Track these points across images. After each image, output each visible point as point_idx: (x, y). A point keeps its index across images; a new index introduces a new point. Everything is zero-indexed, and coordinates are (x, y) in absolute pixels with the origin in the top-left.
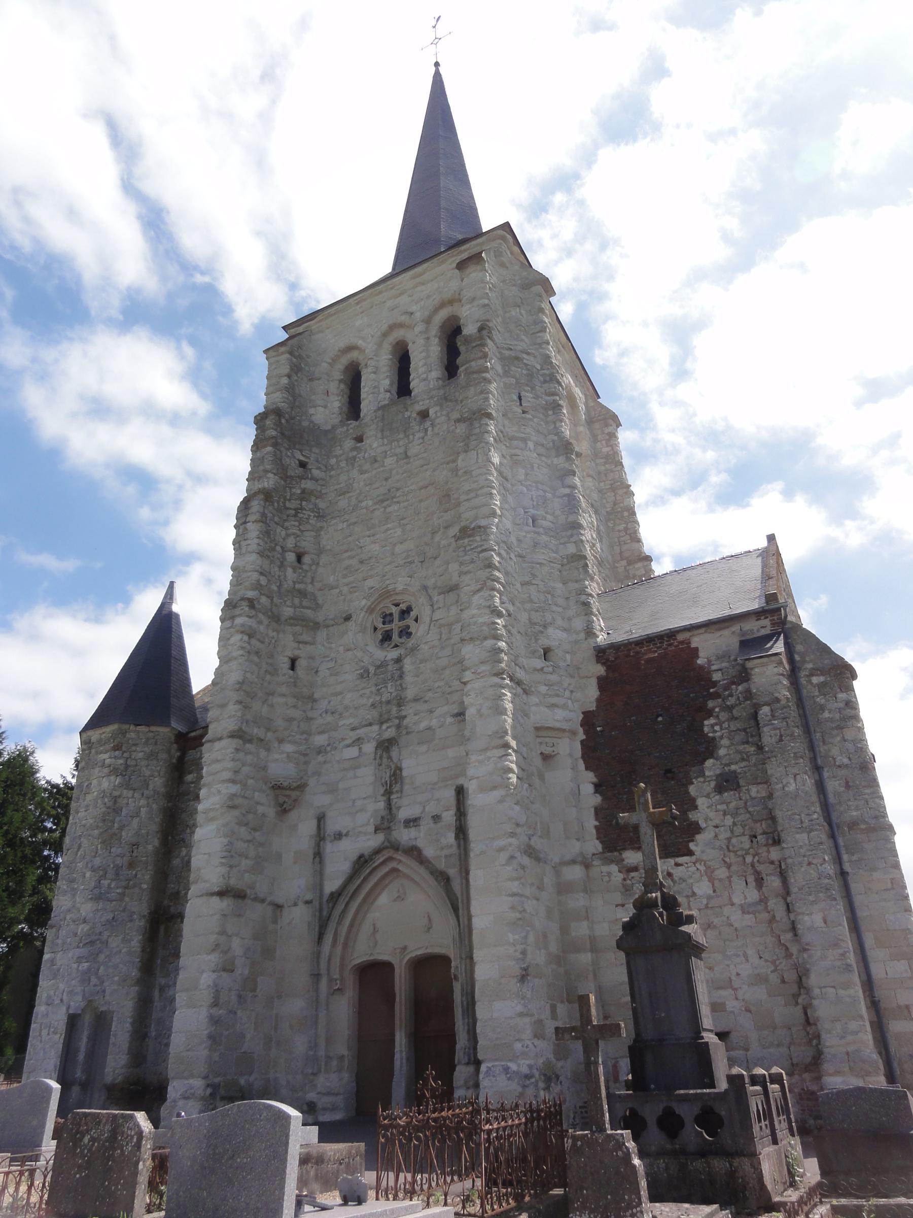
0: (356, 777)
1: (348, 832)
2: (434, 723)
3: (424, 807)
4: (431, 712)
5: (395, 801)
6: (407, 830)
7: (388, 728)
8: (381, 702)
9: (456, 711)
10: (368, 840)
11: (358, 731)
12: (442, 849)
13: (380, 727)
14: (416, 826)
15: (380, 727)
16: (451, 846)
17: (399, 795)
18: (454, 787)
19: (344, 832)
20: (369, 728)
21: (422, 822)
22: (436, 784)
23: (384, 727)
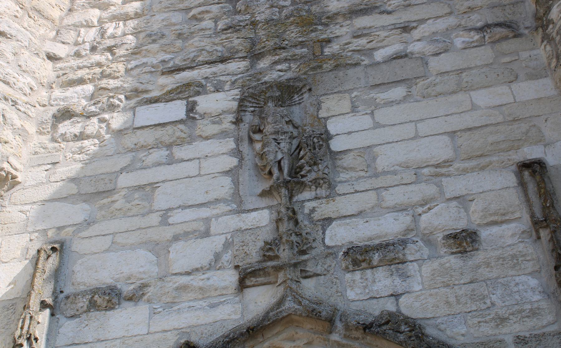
0: (171, 161)
1: (144, 286)
2: (416, 47)
3: (416, 218)
4: (406, 29)
5: (309, 205)
6: (358, 275)
7: (276, 63)
8: (254, 24)
9: (479, 24)
10: (213, 306)
11: (187, 75)
12: (502, 320)
13: (252, 66)
14: (391, 262)
15: (252, 66)
16: (534, 313)
17: (322, 192)
18: (514, 168)
19: (127, 289)
20: (221, 66)
21: (411, 253)
22: (447, 163)
23: (263, 64)
